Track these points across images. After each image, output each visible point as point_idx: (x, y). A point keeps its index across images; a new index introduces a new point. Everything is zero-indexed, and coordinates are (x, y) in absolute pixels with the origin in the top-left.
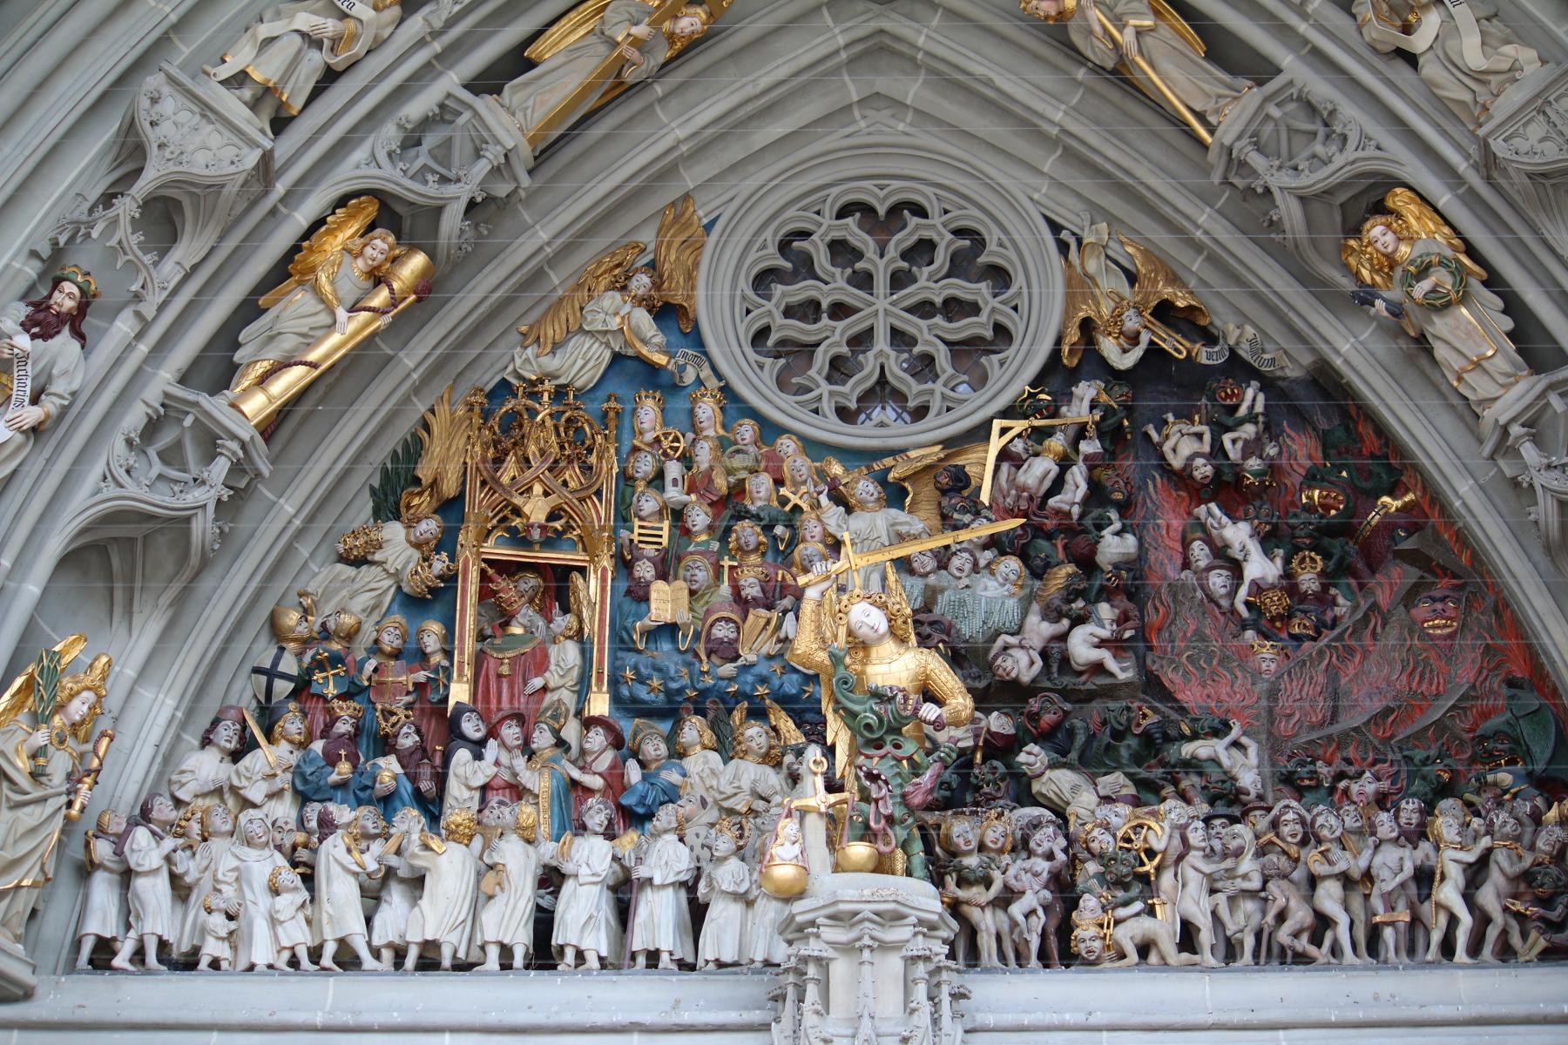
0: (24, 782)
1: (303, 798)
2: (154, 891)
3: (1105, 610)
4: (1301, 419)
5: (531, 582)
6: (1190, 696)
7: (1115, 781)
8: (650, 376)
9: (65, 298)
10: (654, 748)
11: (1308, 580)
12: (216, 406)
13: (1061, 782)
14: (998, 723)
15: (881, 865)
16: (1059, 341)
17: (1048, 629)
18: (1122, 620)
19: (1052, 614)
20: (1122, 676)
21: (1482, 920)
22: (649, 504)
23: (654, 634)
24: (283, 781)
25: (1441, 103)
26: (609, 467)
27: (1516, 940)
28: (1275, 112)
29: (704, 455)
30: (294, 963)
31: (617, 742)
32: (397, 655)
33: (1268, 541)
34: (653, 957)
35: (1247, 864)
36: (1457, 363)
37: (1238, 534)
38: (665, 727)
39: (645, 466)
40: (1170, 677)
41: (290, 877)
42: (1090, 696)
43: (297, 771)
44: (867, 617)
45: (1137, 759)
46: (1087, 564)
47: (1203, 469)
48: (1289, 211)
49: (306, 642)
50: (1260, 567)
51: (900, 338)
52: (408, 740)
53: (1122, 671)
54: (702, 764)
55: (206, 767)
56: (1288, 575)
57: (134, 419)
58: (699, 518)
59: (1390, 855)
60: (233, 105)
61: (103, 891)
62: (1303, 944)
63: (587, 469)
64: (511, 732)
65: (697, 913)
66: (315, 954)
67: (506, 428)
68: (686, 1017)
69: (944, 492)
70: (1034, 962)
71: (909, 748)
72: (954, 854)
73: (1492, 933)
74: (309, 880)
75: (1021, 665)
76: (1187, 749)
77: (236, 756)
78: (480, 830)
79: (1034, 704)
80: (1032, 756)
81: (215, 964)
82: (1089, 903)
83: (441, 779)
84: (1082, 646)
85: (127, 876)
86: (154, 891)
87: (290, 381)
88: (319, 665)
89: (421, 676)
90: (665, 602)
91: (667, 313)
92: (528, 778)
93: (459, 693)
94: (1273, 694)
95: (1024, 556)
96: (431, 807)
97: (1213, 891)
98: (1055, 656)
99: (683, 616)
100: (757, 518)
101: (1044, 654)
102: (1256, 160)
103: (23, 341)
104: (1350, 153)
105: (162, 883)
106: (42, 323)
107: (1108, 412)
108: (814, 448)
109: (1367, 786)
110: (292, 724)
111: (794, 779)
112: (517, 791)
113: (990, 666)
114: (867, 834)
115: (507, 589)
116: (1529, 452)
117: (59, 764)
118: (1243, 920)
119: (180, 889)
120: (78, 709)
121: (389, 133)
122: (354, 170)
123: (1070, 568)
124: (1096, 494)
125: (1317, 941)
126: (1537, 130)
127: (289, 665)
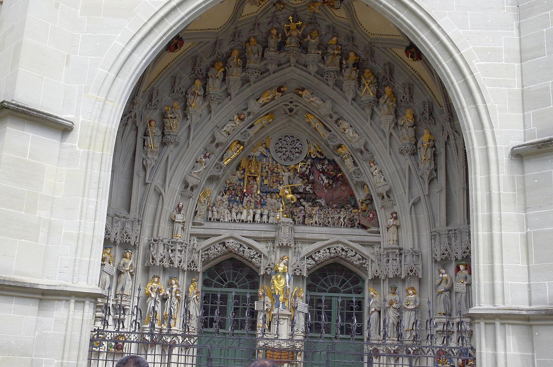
0: (203, 203)
1: (229, 201)
2: (215, 213)
3: (310, 185)
4: (331, 164)
5: (251, 178)
6: (318, 195)
7: (310, 204)
8: (265, 156)
9: (207, 155)
10: (264, 197)
11: (331, 183)
13: (304, 203)
14: (299, 196)
15: (287, 217)
16: (307, 154)
17: (304, 187)
18: (312, 186)
19: (304, 185)
20: (311, 192)
22: (264, 171)
23: (264, 185)
24: (227, 200)
25: (348, 139)
26: (260, 166)
27: (348, 225)
28: (331, 136)
29: (270, 165)
30: (229, 221)
31: (261, 196)
32: (238, 185)
33: (327, 178)
34: (264, 222)
35: (322, 216)
36: (347, 165)
37: (324, 177)
38: (265, 194)
40: (316, 193)
41: (229, 212)
42: (308, 194)
43: (228, 198)
44: (287, 192)
45: (312, 201)
46: (308, 179)
47: (321, 170)
48: (331, 147)
49: (229, 184)
50: (326, 181)
51: (291, 152)
52: (240, 195)
53: (311, 192)
54: (269, 199)
55: (219, 197)
56: (329, 182)
58: (269, 173)
59: (336, 216)
60: (224, 133)
61: (210, 213)
62: (327, 224)
63: (258, 166)
64: (250, 195)
65: (268, 217)
66: (232, 220)
67: (250, 162)
68: (269, 230)
69: (294, 171)
70: (301, 224)
71: (290, 205)
72: (294, 213)
73: (346, 224)
74: (231, 212)
75: (301, 190)
76: (317, 200)
77: (222, 196)
78: (248, 209)
79: (302, 195)
80: (302, 200)
81: (222, 221)
82: (307, 219)
83: (243, 199)
84: (307, 189)
85: (212, 211)
86: (215, 213)
88: (230, 186)
89: (241, 188)
90: (266, 182)
91: (266, 148)
92: (252, 200)
93: (245, 191)
94: (326, 195)
95: (302, 178)
96: (242, 203)
97: (319, 218)
98: (304, 189)
99: (268, 183)
100: (275, 173)
101: (304, 189)
103: (204, 160)
104: (338, 142)
105: (216, 212)
106: (205, 157)
107: (312, 163)
109: (335, 206)
110: (228, 193)
111: (278, 201)
112: (251, 201)
113: (298, 190)
114: (286, 214)
115: (250, 179)
116: (353, 175)
118: (321, 221)
119: (218, 212)
120: (208, 195)
121: (240, 134)
123: (307, 180)
124: (310, 172)
125: (328, 224)
126: (357, 144)
127: (227, 186)
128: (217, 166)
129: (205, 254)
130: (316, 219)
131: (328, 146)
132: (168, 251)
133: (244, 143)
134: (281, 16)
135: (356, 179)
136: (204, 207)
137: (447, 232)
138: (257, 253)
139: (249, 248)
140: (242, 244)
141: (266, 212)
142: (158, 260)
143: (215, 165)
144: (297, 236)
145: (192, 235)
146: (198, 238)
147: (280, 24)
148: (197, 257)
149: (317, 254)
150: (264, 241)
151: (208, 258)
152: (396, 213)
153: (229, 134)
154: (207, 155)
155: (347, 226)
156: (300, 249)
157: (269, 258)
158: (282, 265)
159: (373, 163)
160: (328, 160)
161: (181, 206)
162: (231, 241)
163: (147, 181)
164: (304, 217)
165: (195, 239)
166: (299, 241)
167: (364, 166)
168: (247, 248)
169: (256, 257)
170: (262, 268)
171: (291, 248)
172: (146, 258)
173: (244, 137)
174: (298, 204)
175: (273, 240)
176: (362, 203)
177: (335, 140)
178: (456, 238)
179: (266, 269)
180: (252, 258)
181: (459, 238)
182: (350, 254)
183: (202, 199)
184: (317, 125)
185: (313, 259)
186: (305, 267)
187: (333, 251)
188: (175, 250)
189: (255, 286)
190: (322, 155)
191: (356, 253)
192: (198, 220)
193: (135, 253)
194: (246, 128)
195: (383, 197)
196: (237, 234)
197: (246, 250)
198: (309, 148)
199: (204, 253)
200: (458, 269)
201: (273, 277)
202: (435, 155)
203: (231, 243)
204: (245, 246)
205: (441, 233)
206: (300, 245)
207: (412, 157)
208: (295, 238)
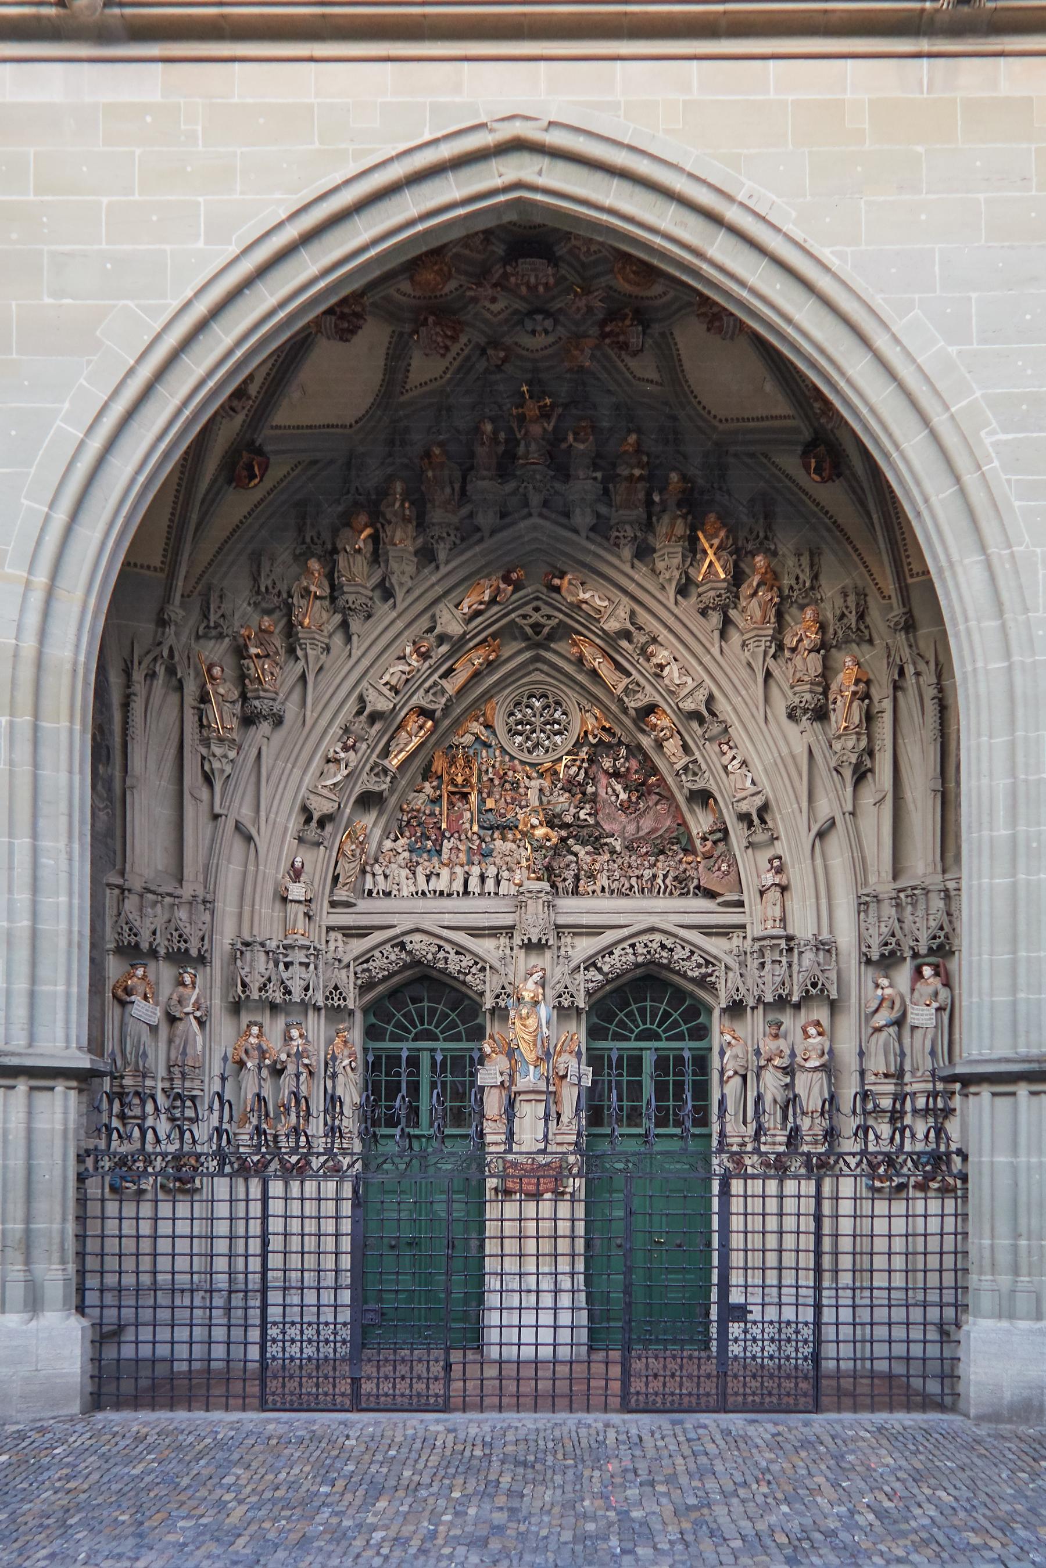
12: (386, 763)
21: (666, 887)
39: (484, 768)
57: (367, 768)
87: (402, 756)
102: (626, 699)
108: (522, 763)
117: (358, 851)
121: (422, 691)
122: (414, 701)
128: (376, 770)
129: (364, 971)
130: (603, 880)
131: (625, 710)
132: (276, 965)
133: (434, 711)
134: (501, 387)
135: (689, 785)
136: (352, 865)
137: (894, 894)
138: (476, 963)
139: (457, 953)
140: (442, 943)
141: (492, 871)
142: (254, 987)
143: (372, 769)
144: (562, 920)
145: (330, 929)
146: (344, 935)
147: (500, 407)
148: (344, 977)
149: (607, 959)
150: (490, 936)
151: (370, 977)
152: (780, 858)
153: (397, 693)
154: (350, 742)
155: (671, 893)
156: (569, 949)
157: (503, 972)
158: (530, 984)
159: (727, 743)
160: (627, 746)
161: (298, 865)
162: (417, 937)
163: (217, 810)
164: (577, 878)
165: (340, 936)
166: (566, 931)
167: (708, 755)
168: (452, 952)
169: (474, 970)
170: (488, 994)
171: (549, 947)
172: (230, 983)
173: (431, 697)
174: (562, 847)
175: (509, 930)
176: (704, 839)
177: (639, 696)
178: (914, 905)
179: (497, 997)
180: (466, 974)
181: (921, 906)
182: (680, 954)
183: (349, 848)
184: (599, 663)
185: (599, 970)
186: (581, 986)
187: (641, 950)
188: (292, 963)
189: (478, 1033)
190: (614, 735)
191: (692, 953)
192: (341, 894)
193: (204, 972)
194: (435, 677)
195: (751, 824)
196: (427, 923)
197: (452, 956)
198: (583, 722)
199: (359, 969)
200: (918, 972)
201: (512, 1013)
202: (869, 717)
203: (418, 944)
204: (448, 947)
205: (881, 896)
206: (569, 940)
207: (817, 725)
208: (557, 926)
